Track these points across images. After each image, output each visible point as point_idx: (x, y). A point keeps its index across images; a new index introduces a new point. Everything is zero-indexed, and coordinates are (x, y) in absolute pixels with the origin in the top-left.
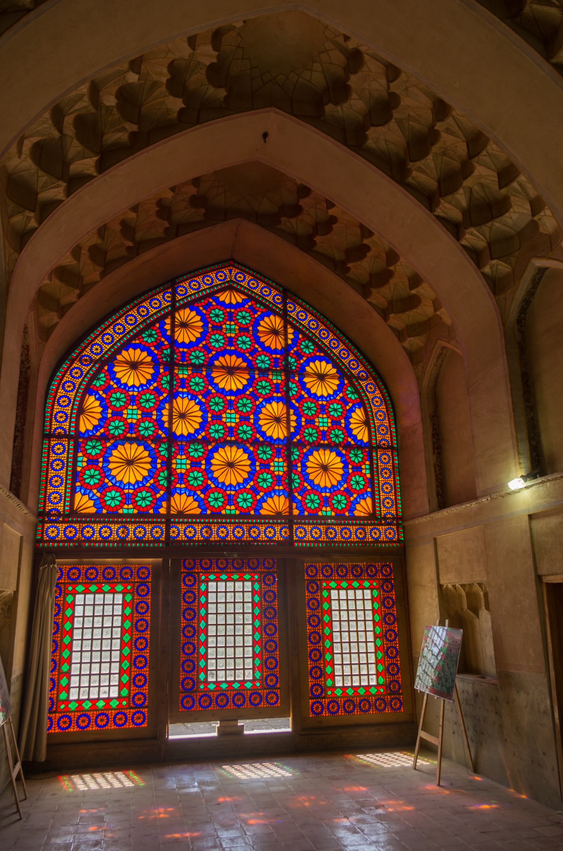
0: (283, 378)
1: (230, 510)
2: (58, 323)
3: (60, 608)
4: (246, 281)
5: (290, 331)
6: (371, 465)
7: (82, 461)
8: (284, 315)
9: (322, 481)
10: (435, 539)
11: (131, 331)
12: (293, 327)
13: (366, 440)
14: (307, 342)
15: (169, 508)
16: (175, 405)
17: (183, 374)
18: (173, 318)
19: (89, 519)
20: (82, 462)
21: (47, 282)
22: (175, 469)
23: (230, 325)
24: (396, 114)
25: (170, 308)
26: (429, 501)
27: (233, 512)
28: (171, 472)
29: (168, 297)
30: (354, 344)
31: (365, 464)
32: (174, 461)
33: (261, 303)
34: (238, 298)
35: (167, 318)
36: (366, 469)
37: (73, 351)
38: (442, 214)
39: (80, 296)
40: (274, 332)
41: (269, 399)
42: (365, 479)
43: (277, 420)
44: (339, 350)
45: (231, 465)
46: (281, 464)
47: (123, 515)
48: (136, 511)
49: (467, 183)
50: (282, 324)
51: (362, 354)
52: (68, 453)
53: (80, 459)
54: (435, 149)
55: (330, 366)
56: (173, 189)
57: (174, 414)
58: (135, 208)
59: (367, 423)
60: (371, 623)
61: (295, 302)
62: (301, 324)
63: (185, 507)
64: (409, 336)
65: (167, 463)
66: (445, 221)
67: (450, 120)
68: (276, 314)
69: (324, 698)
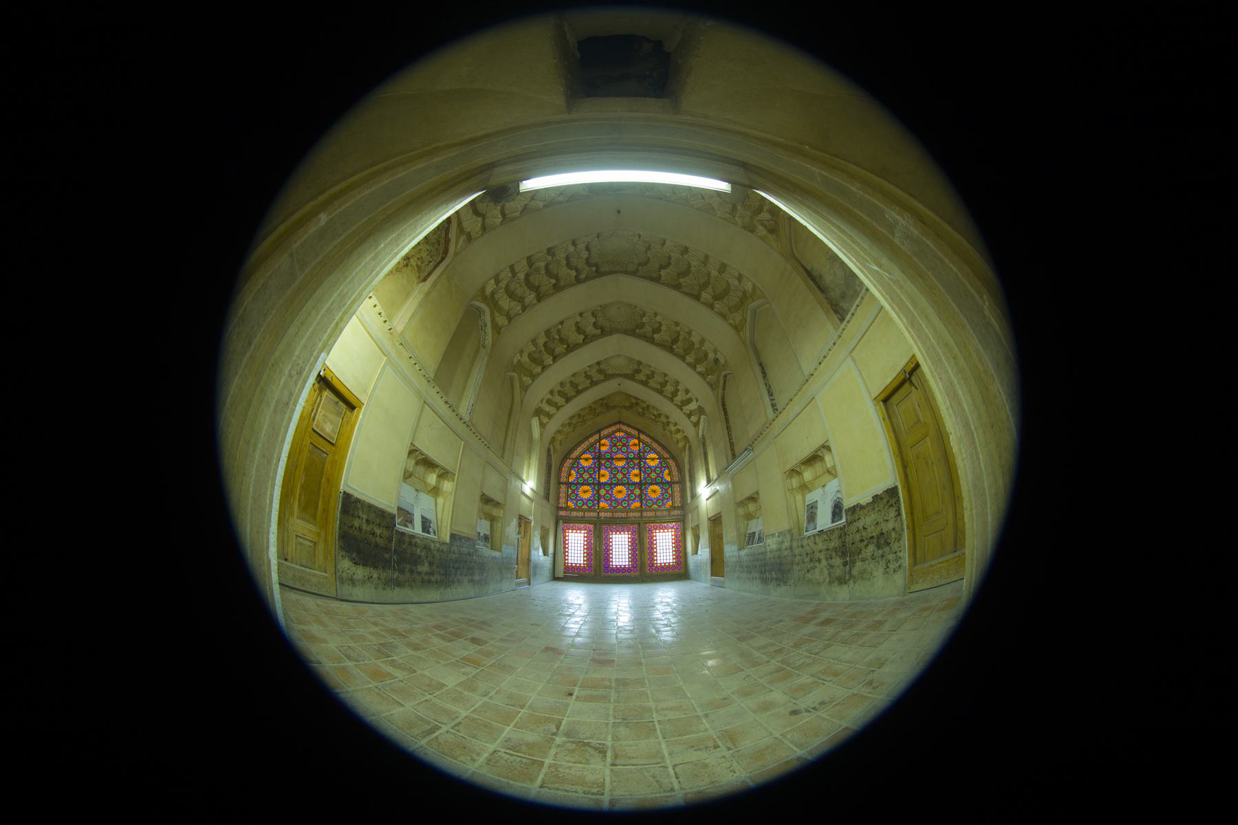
3: (564, 537)
4: (625, 428)
8: (639, 438)
9: (653, 496)
15: (598, 506)
18: (600, 443)
19: (572, 510)
20: (570, 492)
28: (599, 495)
34: (622, 434)
36: (670, 491)
40: (635, 445)
41: (633, 468)
43: (636, 475)
44: (659, 449)
45: (620, 492)
59: (669, 474)
65: (598, 491)
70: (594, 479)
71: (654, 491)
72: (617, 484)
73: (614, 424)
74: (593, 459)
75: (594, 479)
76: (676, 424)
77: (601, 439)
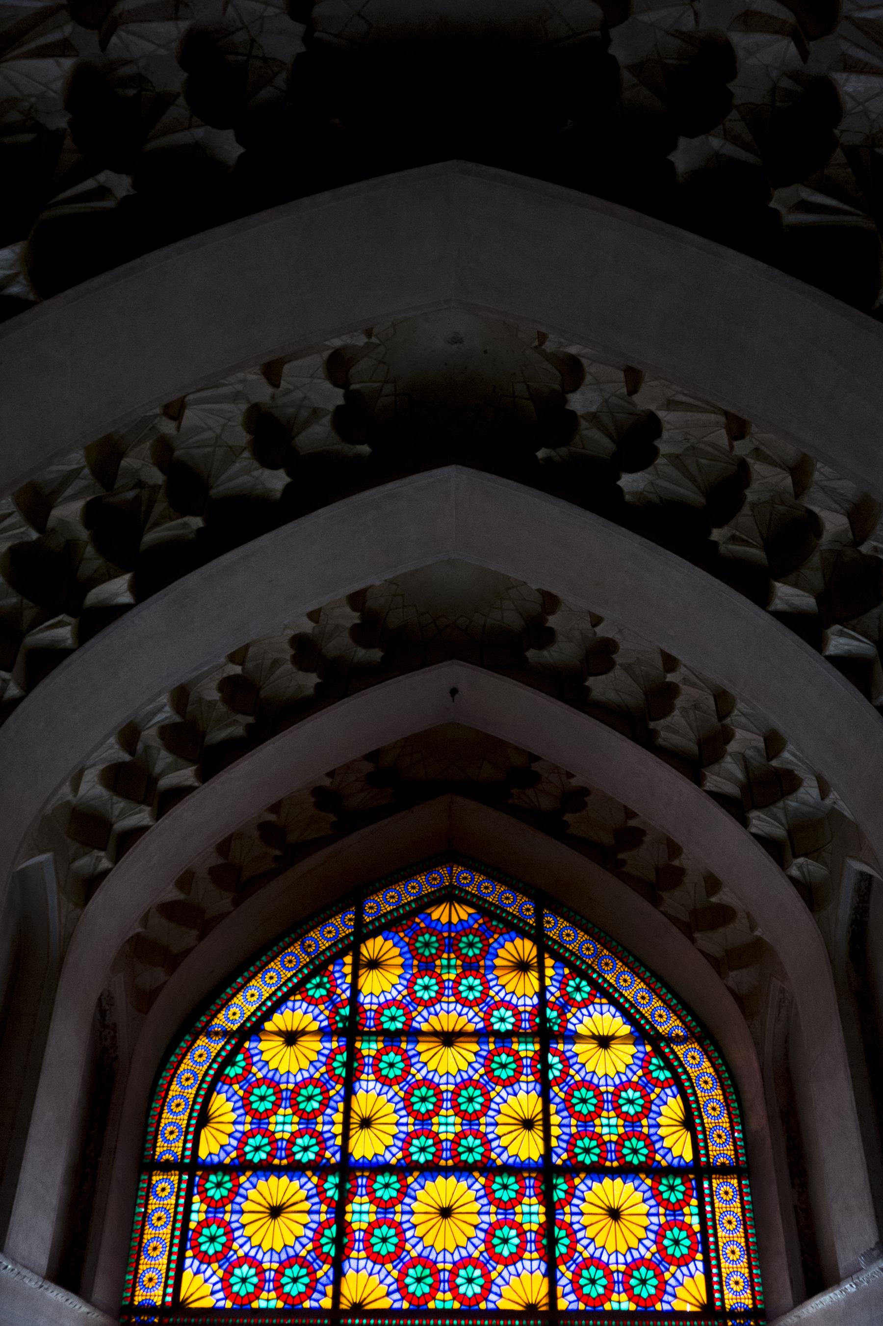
1: (444, 1301)
2: (165, 983)
5: (549, 962)
7: (198, 1212)
11: (290, 979)
12: (555, 956)
14: (578, 980)
15: (337, 1295)
17: (369, 1048)
18: (357, 955)
20: (199, 1211)
21: (139, 930)
23: (449, 959)
24: (619, 659)
25: (352, 938)
28: (344, 1228)
29: (350, 920)
30: (659, 979)
32: (349, 1208)
35: (346, 954)
37: (198, 1019)
38: (714, 789)
39: (201, 938)
42: (691, 1235)
43: (528, 1124)
46: (534, 1209)
48: (280, 1304)
49: (732, 747)
50: (534, 952)
51: (675, 995)
52: (178, 1197)
53: (195, 1207)
54: (679, 702)
55: (619, 1020)
56: (331, 774)
57: (352, 1121)
58: (275, 808)
61: (556, 913)
62: (567, 950)
63: (364, 1296)
64: (731, 969)
65: (339, 1209)
66: (719, 798)
67: (683, 670)
68: (523, 935)
70: (322, 1141)
71: (615, 1214)
72: (431, 1170)
73: (426, 866)
74: (325, 1033)
75: (322, 1141)
76: (713, 884)
77: (362, 934)
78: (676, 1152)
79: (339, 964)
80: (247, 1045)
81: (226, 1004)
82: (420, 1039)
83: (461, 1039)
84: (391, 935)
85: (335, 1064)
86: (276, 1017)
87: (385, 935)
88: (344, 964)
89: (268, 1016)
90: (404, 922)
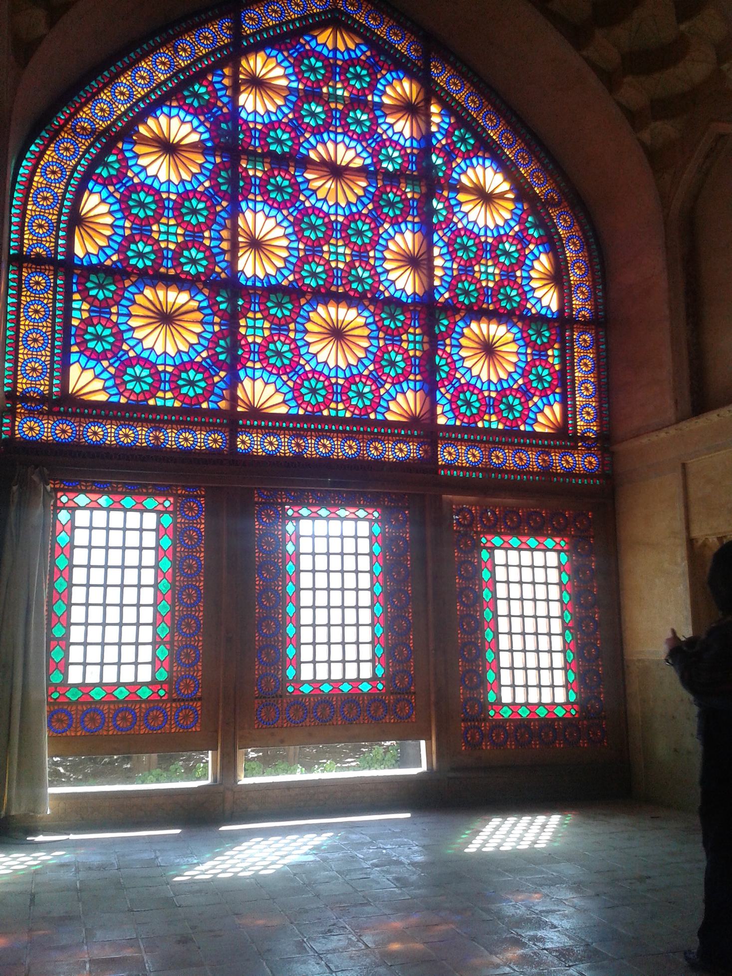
0: (424, 190)
5: (434, 109)
6: (562, 350)
10: (684, 465)
13: (554, 307)
16: (241, 222)
18: (236, 66)
20: (80, 309)
22: (245, 337)
26: (676, 402)
27: (341, 414)
31: (553, 348)
33: (387, 53)
35: (225, 66)
47: (155, 408)
52: (55, 293)
55: (500, 177)
59: (558, 277)
60: (558, 604)
69: (484, 720)
70: (211, 256)
72: (324, 296)
78: (545, 302)
79: (219, 75)
80: (120, 145)
81: (93, 97)
82: (308, 166)
83: (347, 173)
84: (274, 53)
85: (220, 180)
86: (151, 122)
87: (268, 51)
88: (224, 76)
89: (141, 118)
90: (288, 41)
